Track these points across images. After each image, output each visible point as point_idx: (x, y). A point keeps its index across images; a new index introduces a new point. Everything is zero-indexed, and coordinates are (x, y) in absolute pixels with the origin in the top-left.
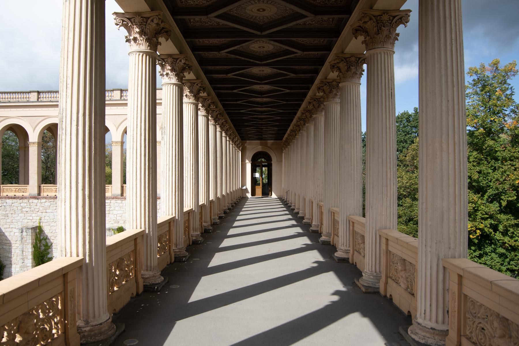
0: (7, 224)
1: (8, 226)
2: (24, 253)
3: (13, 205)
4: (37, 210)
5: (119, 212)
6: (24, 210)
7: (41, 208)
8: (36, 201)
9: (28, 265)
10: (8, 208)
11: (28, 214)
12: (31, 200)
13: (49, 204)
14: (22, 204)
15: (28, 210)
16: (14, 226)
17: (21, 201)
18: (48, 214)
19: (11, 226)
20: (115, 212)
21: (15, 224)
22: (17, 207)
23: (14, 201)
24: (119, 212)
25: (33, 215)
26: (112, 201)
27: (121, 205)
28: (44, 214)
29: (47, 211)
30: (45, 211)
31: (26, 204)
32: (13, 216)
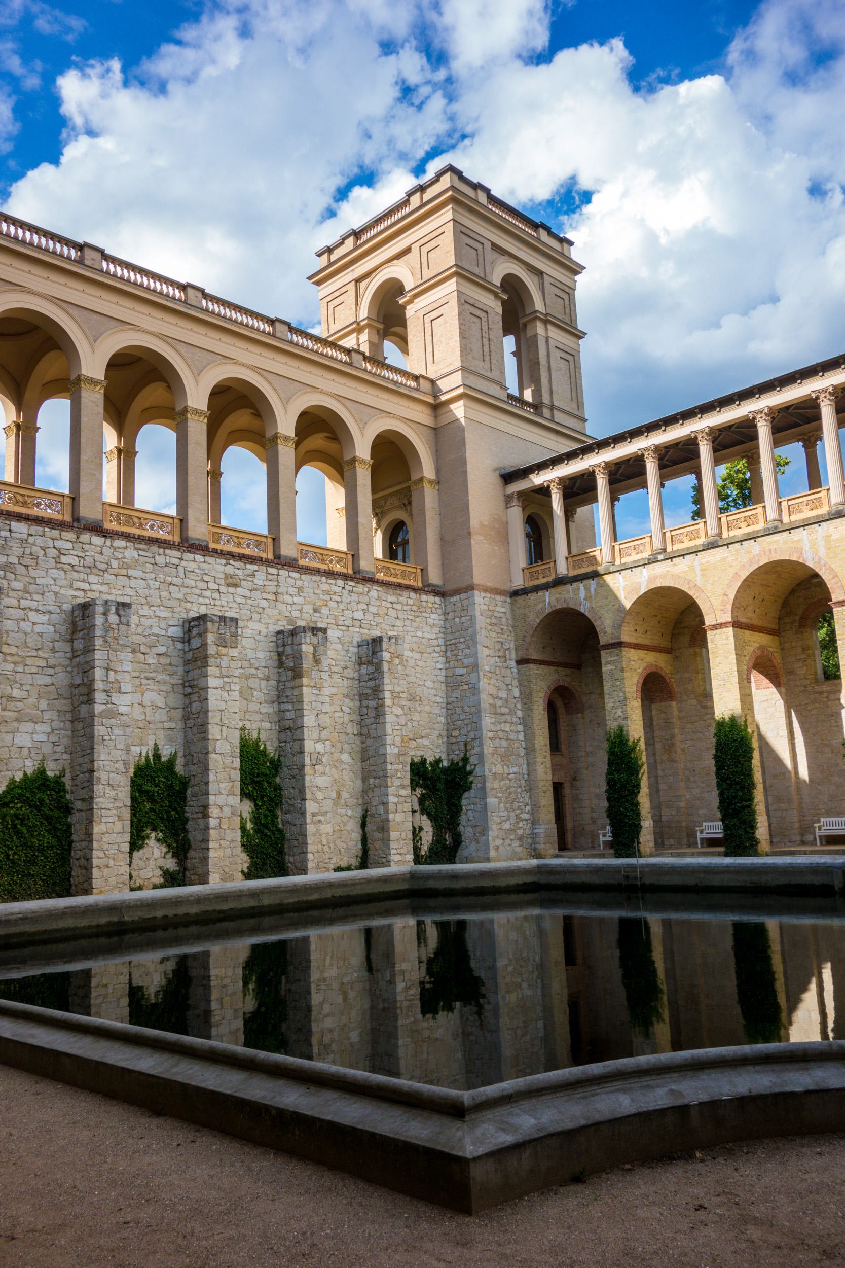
0: (11, 594)
1: (14, 602)
2: (111, 673)
3: (31, 540)
4: (104, 567)
5: (296, 600)
6: (63, 559)
7: (115, 564)
8: (98, 540)
9: (122, 709)
10: (17, 550)
11: (75, 575)
12: (85, 537)
13: (135, 554)
14: (58, 544)
15: (75, 561)
16: (34, 604)
17: (55, 533)
18: (133, 583)
19: (24, 603)
20: (288, 599)
21: (35, 597)
22: (43, 549)
23: (35, 529)
24: (296, 600)
25: (93, 579)
26: (282, 572)
27: (299, 583)
28: (122, 581)
29: (131, 572)
30: (124, 572)
31: (69, 545)
32: (33, 573)
